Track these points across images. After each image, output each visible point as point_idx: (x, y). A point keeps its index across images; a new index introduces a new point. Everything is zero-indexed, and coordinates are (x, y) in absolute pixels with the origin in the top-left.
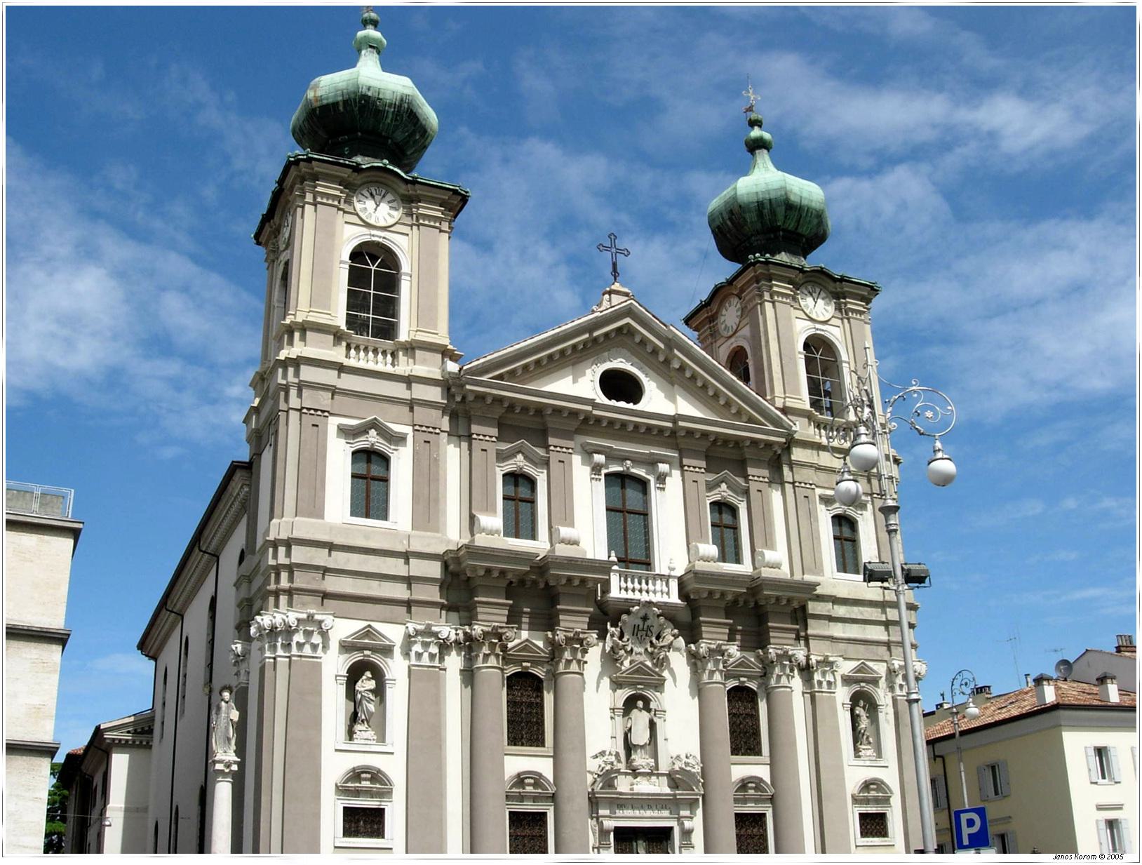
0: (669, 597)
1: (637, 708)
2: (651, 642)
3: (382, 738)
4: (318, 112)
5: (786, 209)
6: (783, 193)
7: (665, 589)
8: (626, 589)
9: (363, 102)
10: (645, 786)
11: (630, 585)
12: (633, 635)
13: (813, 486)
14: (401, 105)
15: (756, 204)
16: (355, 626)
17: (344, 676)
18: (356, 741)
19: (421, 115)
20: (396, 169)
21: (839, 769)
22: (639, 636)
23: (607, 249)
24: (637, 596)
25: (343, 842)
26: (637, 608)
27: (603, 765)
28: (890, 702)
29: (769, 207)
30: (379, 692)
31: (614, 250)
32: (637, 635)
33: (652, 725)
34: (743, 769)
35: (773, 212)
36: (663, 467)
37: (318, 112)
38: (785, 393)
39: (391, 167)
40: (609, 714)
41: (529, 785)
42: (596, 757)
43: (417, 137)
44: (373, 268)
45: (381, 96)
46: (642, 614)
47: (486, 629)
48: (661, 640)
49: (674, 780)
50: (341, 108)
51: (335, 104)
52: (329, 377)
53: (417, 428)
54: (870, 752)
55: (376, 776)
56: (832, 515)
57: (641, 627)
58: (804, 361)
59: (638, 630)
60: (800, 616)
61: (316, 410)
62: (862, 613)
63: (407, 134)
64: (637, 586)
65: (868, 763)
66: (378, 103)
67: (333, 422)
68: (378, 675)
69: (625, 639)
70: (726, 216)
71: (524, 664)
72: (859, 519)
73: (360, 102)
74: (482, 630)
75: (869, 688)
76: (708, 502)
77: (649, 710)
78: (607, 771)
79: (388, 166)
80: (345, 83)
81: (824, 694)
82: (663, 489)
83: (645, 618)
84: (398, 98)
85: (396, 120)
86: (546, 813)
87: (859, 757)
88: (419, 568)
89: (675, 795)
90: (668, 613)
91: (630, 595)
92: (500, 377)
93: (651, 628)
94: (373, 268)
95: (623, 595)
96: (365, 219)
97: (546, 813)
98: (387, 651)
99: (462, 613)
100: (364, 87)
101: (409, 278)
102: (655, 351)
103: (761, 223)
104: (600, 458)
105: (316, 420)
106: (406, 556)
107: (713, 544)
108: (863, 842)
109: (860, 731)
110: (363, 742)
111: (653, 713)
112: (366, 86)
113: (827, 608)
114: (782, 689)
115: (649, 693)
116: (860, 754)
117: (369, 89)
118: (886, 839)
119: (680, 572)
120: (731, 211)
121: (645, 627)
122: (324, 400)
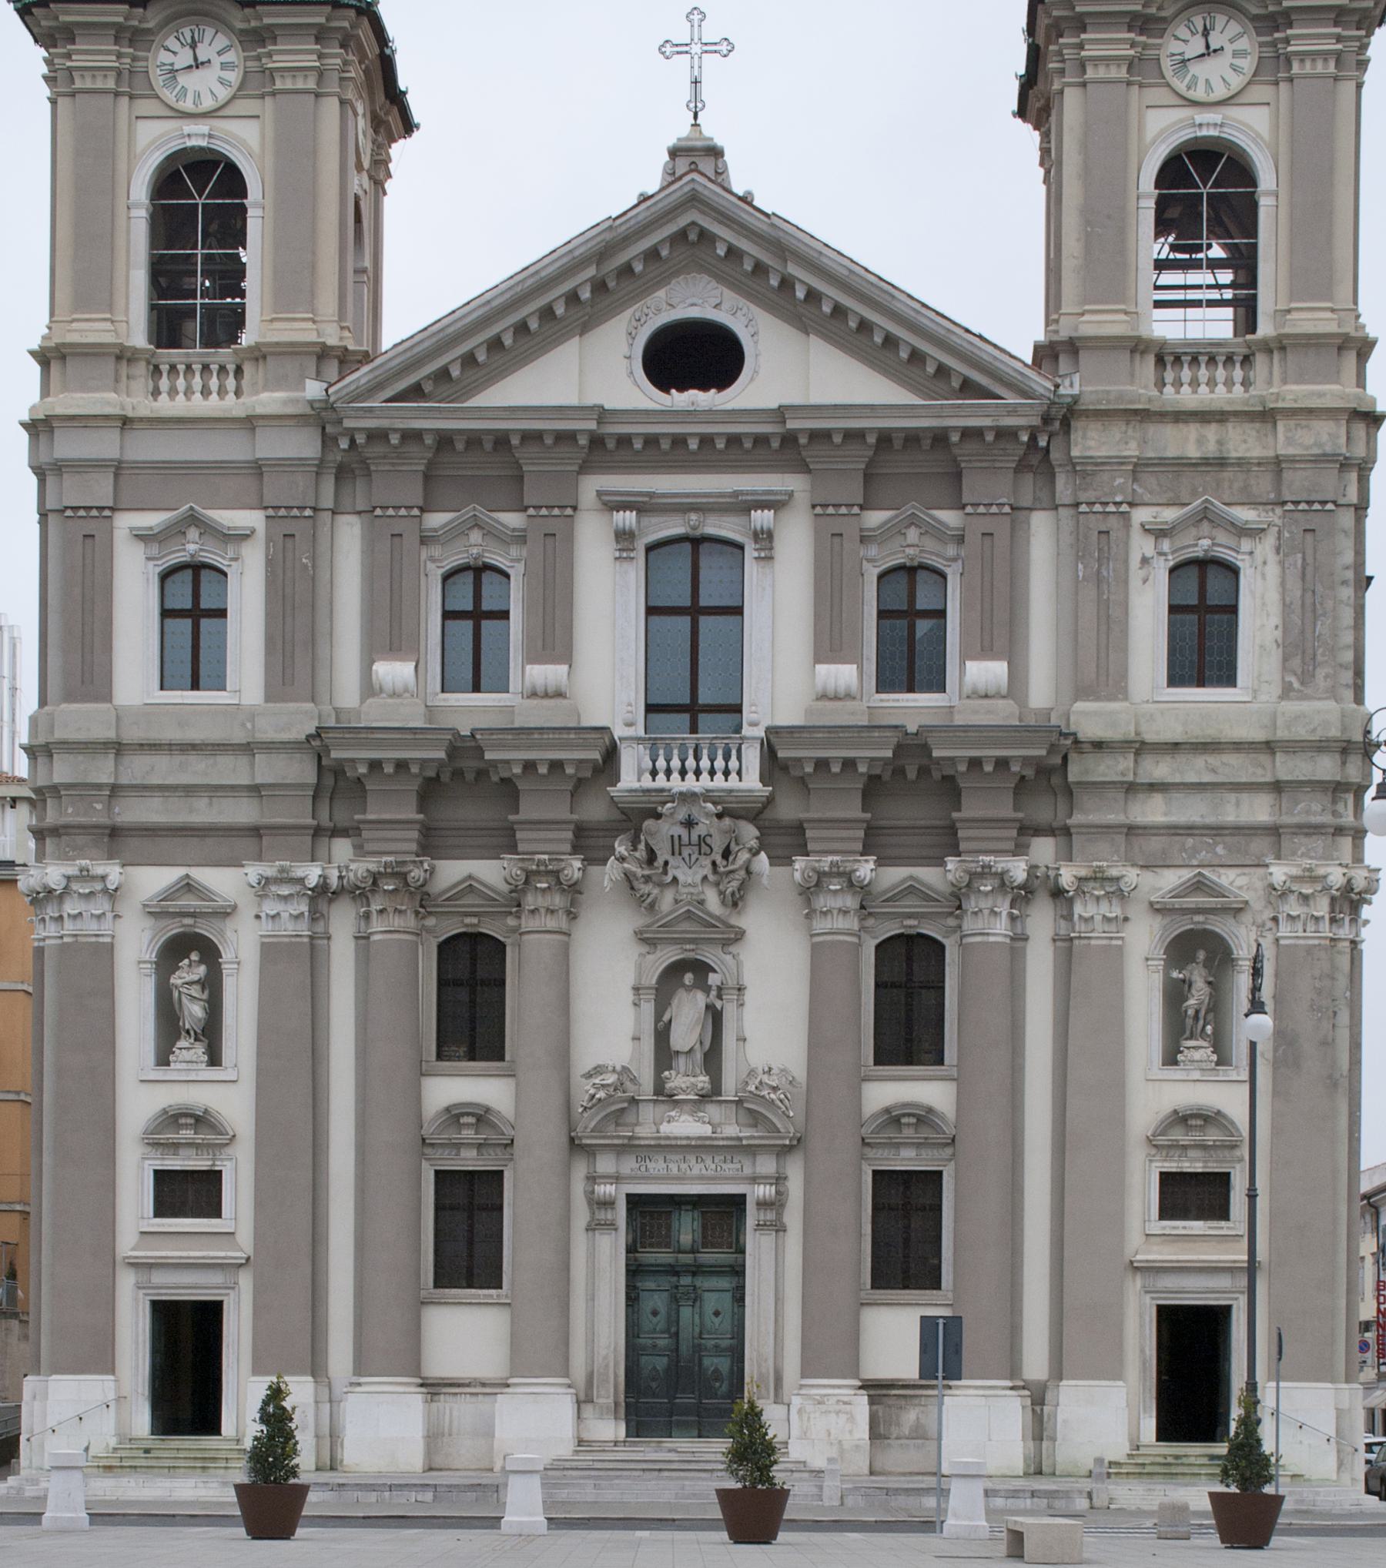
0: (740, 780)
1: (683, 985)
3: (214, 1059)
10: (685, 1126)
12: (673, 854)
13: (1124, 508)
17: (150, 962)
21: (1115, 1087)
22: (685, 854)
23: (681, 49)
25: (153, 1225)
26: (669, 805)
27: (592, 1091)
30: (212, 986)
32: (680, 854)
33: (715, 1017)
36: (762, 518)
40: (630, 996)
41: (468, 1125)
42: (589, 1076)
44: (200, 202)
46: (681, 815)
47: (373, 867)
48: (731, 858)
49: (751, 1109)
53: (271, 512)
55: (201, 1120)
57: (685, 839)
58: (1152, 213)
59: (680, 845)
61: (88, 508)
62: (1214, 771)
65: (1196, 1075)
68: (210, 953)
69: (660, 862)
71: (468, 920)
72: (1243, 563)
74: (368, 871)
76: (872, 573)
77: (707, 989)
78: (600, 1100)
81: (1093, 942)
82: (770, 558)
83: (689, 824)
86: (502, 1171)
87: (1175, 1063)
88: (267, 770)
89: (740, 1139)
90: (731, 809)
93: (708, 840)
95: (647, 782)
97: (502, 1171)
98: (226, 913)
102: (760, 269)
104: (628, 518)
105: (90, 527)
106: (248, 749)
108: (1164, 1228)
109: (1186, 1011)
110: (184, 1066)
111: (714, 993)
113: (1121, 767)
114: (978, 939)
115: (710, 955)
116: (1180, 1057)
118: (1223, 1223)
122: (101, 490)
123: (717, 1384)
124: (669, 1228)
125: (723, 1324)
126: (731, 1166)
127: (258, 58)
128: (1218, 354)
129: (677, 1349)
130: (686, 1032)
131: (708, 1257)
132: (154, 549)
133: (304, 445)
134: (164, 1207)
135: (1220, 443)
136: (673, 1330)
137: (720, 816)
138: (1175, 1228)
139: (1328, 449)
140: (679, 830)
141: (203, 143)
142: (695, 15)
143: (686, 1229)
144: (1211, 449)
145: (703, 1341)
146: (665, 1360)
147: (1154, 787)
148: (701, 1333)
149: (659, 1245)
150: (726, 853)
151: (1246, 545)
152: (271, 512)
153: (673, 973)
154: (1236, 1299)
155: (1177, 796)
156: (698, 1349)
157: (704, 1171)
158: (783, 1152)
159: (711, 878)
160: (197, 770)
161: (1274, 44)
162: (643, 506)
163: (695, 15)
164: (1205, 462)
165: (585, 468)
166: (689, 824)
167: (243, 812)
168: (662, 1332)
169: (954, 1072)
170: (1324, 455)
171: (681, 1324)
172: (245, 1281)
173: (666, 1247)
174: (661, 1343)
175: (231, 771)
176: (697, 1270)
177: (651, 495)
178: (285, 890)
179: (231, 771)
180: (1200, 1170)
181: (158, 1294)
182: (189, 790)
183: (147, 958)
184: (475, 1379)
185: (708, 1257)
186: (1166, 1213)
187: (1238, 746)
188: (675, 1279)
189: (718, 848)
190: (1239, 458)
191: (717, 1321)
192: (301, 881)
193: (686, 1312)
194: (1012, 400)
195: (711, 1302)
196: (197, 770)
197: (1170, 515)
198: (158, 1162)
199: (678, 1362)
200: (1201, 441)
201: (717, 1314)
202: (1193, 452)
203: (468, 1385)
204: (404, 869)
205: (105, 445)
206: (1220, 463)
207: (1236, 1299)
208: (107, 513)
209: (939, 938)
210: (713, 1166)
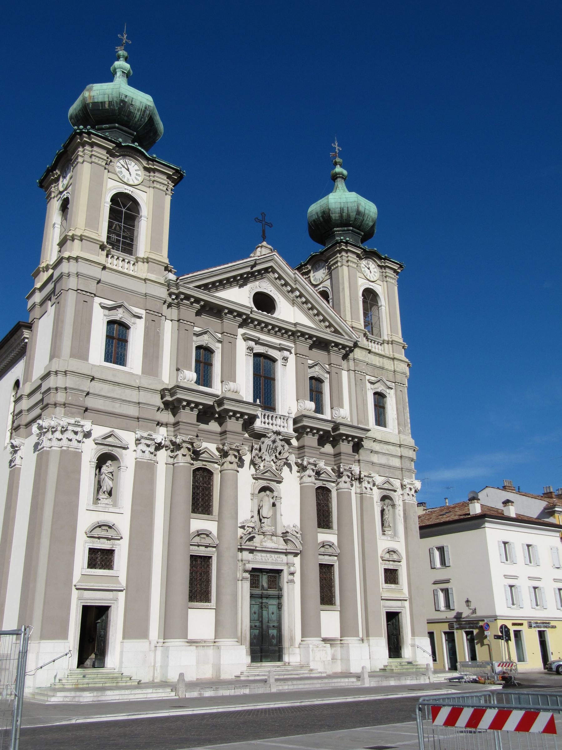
2: (276, 456)
3: (115, 505)
4: (90, 106)
5: (356, 214)
6: (356, 205)
7: (286, 425)
8: (265, 423)
9: (122, 105)
10: (269, 544)
11: (267, 421)
13: (365, 374)
14: (145, 111)
15: (339, 209)
16: (106, 430)
18: (99, 505)
19: (156, 121)
20: (142, 150)
24: (270, 427)
28: (401, 503)
29: (346, 212)
31: (264, 222)
34: (324, 536)
35: (348, 215)
36: (286, 353)
37: (90, 106)
38: (352, 319)
39: (140, 148)
40: (250, 497)
43: (152, 135)
45: (133, 103)
46: (272, 438)
48: (281, 455)
50: (107, 106)
51: (103, 103)
52: (96, 272)
53: (148, 311)
54: (390, 533)
56: (374, 392)
60: (357, 446)
63: (146, 131)
64: (271, 422)
66: (131, 107)
67: (97, 300)
70: (320, 215)
73: (120, 104)
75: (391, 494)
79: (138, 147)
80: (110, 90)
83: (274, 442)
84: (144, 106)
85: (141, 120)
88: (144, 397)
91: (266, 426)
92: (199, 287)
94: (124, 210)
95: (263, 425)
96: (121, 178)
99: (170, 429)
100: (123, 95)
101: (146, 219)
103: (341, 220)
104: (252, 344)
107: (311, 400)
110: (104, 505)
112: (124, 94)
115: (273, 485)
117: (126, 96)
118: (398, 585)
119: (293, 416)
120: (324, 211)
121: (274, 448)
122: (92, 287)
123: (273, 640)
124: (258, 580)
125: (274, 617)
126: (279, 559)
127: (149, 176)
128: (376, 341)
129: (262, 627)
130: (265, 512)
131: (272, 592)
132: (107, 312)
133: (163, 293)
134: (92, 564)
135: (383, 363)
136: (260, 619)
137: (281, 440)
138: (388, 586)
139: (404, 371)
140: (270, 443)
141: (130, 193)
142: (263, 214)
143: (264, 580)
144: (381, 365)
145: (269, 624)
146: (258, 631)
147: (377, 452)
148: (268, 621)
149: (256, 587)
150: (280, 453)
151: (388, 391)
152: (148, 311)
153: (264, 489)
154: (402, 610)
155: (380, 456)
156: (268, 627)
157: (272, 561)
158: (296, 555)
159: (275, 460)
160: (118, 392)
161: (382, 272)
162: (257, 342)
163: (263, 214)
164: (380, 367)
165: (240, 326)
166: (274, 442)
167: (133, 411)
168: (257, 621)
169: (336, 532)
170: (403, 372)
171: (263, 617)
172: (122, 596)
173: (258, 588)
174: (256, 624)
175: (134, 396)
176: (268, 597)
177: (259, 339)
178: (148, 442)
179: (134, 396)
180: (392, 568)
181: (87, 603)
182: (114, 399)
183: (93, 460)
184: (202, 640)
185: (272, 592)
186: (386, 582)
187: (393, 444)
188: (261, 600)
189: (278, 452)
190: (387, 368)
191: (273, 616)
192: (153, 440)
193: (265, 613)
194: (347, 337)
195: (273, 608)
196: (118, 392)
197: (373, 378)
198: (91, 544)
199: (262, 632)
200: (379, 362)
201: (273, 613)
202: (378, 364)
203: (200, 642)
204: (193, 441)
205: (96, 272)
206: (383, 368)
207: (402, 610)
208: (93, 295)
209: (330, 489)
210: (275, 559)
